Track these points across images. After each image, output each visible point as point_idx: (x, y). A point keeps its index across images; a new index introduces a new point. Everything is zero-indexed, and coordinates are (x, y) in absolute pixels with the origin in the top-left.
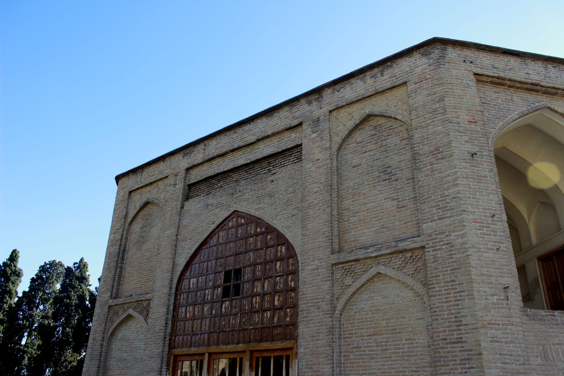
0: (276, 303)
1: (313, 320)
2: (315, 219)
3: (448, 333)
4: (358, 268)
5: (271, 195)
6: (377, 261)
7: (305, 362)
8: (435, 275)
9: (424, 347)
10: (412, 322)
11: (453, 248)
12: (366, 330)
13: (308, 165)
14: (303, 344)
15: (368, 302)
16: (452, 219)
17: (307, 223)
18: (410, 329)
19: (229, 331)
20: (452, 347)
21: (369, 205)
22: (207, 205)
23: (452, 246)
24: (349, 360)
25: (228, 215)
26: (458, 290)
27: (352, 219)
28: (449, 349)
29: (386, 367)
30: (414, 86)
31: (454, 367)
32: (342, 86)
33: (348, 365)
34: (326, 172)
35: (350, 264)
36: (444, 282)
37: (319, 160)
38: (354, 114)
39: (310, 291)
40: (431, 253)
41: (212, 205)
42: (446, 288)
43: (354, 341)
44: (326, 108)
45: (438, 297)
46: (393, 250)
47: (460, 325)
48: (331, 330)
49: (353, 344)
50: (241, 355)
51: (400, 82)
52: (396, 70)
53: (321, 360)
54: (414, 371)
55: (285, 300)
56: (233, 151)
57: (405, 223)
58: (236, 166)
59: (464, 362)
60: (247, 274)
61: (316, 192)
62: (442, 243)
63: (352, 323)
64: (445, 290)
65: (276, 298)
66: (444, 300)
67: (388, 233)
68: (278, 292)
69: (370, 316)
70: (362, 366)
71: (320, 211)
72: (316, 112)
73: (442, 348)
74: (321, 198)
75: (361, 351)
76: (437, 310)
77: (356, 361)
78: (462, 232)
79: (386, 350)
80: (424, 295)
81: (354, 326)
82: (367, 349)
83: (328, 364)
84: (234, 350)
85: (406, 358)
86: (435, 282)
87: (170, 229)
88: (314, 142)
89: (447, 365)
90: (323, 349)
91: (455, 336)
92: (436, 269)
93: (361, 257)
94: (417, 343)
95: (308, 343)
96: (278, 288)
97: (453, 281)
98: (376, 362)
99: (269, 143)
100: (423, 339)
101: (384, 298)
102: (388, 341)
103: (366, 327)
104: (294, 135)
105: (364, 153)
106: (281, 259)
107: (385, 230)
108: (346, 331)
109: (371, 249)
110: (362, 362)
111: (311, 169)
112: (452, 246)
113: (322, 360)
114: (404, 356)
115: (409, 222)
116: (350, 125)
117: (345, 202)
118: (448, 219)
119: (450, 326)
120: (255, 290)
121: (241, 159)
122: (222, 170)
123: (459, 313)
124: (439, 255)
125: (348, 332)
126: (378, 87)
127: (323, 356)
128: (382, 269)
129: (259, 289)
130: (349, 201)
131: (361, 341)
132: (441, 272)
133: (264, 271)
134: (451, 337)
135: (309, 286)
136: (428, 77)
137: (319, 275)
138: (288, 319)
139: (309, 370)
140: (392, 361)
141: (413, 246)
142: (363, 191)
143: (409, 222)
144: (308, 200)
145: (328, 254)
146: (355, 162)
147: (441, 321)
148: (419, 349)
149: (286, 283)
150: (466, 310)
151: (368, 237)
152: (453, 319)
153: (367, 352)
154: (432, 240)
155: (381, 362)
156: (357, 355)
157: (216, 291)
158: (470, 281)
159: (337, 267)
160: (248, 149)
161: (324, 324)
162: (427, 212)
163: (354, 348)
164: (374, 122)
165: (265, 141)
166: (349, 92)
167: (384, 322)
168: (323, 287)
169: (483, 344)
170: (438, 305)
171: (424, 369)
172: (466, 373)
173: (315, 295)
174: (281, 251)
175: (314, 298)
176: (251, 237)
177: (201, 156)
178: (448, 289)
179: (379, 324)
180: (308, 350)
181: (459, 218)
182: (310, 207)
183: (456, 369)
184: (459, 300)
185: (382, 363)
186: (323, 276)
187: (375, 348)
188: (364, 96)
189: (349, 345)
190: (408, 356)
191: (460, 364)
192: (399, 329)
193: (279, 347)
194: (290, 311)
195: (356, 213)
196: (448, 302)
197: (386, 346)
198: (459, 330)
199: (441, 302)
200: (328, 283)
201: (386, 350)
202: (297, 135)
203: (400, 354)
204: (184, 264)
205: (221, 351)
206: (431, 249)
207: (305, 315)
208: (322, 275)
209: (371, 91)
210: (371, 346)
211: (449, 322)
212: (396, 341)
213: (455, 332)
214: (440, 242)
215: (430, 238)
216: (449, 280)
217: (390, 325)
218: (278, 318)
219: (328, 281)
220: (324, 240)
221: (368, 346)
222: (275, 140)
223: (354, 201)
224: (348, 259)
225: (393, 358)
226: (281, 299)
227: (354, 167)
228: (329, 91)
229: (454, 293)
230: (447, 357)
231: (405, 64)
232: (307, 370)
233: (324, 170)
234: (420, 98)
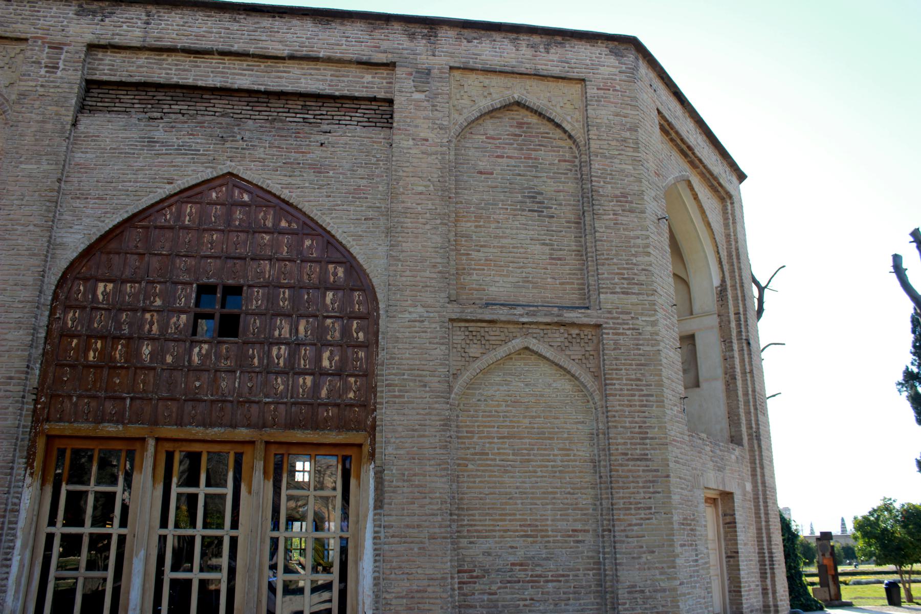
0: (326, 363)
1: (413, 403)
2: (417, 237)
3: (629, 446)
4: (492, 333)
5: (318, 169)
6: (524, 330)
7: (397, 470)
8: (615, 367)
9: (585, 461)
10: (568, 426)
11: (641, 337)
12: (496, 429)
13: (405, 143)
14: (393, 440)
15: (501, 388)
16: (641, 297)
17: (400, 239)
18: (566, 435)
19: (212, 402)
20: (634, 465)
21: (504, 241)
22: (152, 142)
23: (640, 334)
24: (467, 471)
25: (210, 176)
26: (645, 392)
27: (474, 254)
28: (630, 467)
29: (527, 485)
30: (595, 91)
31: (636, 490)
32: (475, 35)
33: (465, 479)
34: (439, 166)
35: (479, 324)
36: (627, 380)
37: (427, 140)
38: (492, 90)
39: (407, 355)
40: (610, 336)
41: (164, 144)
42: (629, 387)
43: (476, 444)
44: (442, 61)
45: (618, 397)
46: (556, 319)
47: (646, 438)
48: (446, 424)
49: (475, 448)
50: (239, 449)
51: (575, 75)
52: (570, 55)
53: (428, 468)
54: (569, 493)
55: (343, 360)
56: (223, 53)
57: (561, 284)
58: (228, 85)
59: (648, 484)
60: (256, 300)
61: (421, 193)
62: (626, 327)
63: (473, 416)
64: (628, 390)
65: (326, 355)
66: (626, 403)
67: (535, 291)
68: (331, 345)
69: (503, 408)
70: (489, 482)
71: (428, 227)
72: (423, 57)
73: (621, 465)
74: (430, 206)
75: (487, 460)
76: (617, 414)
77: (479, 473)
78: (653, 319)
79: (529, 461)
80: (594, 391)
81: (476, 421)
82: (498, 458)
83: (442, 476)
84: (226, 437)
85: (557, 474)
86: (614, 376)
87: (38, 163)
88: (418, 107)
89: (628, 488)
90: (432, 452)
91: (638, 451)
92: (617, 359)
93: (503, 318)
94: (574, 455)
95: (403, 440)
96: (329, 338)
97: (639, 380)
98: (512, 477)
99: (313, 72)
100: (583, 451)
101: (527, 385)
102: (533, 449)
103: (496, 425)
104: (368, 78)
105: (498, 157)
106: (335, 288)
107: (531, 285)
108: (462, 427)
109: (519, 311)
110: (490, 476)
111: (411, 151)
112: (640, 334)
113: (431, 469)
114: (555, 472)
115: (568, 283)
116: (485, 104)
117: (463, 224)
118: (634, 296)
119: (633, 438)
120: (277, 333)
121: (243, 77)
122: (190, 81)
123: (645, 422)
124: (621, 342)
125: (465, 429)
126: (539, 67)
127: (432, 462)
128: (533, 344)
129: (286, 333)
130: (469, 224)
131: (487, 445)
132: (624, 364)
133: (293, 300)
134: (634, 452)
135: (407, 346)
136: (618, 88)
137: (426, 332)
138: (351, 395)
139: (406, 484)
140: (538, 477)
141: (585, 320)
142: (495, 217)
143: (568, 283)
144: (403, 202)
145: (442, 301)
146: (483, 165)
147: (620, 429)
148: (578, 463)
149: (346, 331)
150: (653, 420)
151: (501, 289)
152: (637, 430)
153: (498, 462)
154: (612, 318)
155: (521, 477)
156: (479, 465)
157: (175, 319)
158: (660, 385)
159: (455, 324)
160: (263, 65)
161: (434, 412)
162: (607, 279)
163: (476, 454)
164: (522, 115)
165: (305, 65)
166: (488, 51)
167: (527, 421)
168: (433, 352)
169: (672, 465)
170: (618, 408)
171: (583, 491)
172: (650, 498)
173: (417, 362)
174: (335, 274)
175: (416, 367)
176: (265, 233)
177: (138, 33)
178: (632, 390)
179: (518, 422)
180: (402, 452)
181: (651, 298)
182: (409, 215)
183: (638, 493)
184: (645, 406)
185: (520, 480)
186: (432, 335)
187: (511, 457)
188: (516, 70)
189: (468, 448)
190: (560, 472)
191: (644, 487)
192: (550, 433)
193: (333, 441)
194: (356, 382)
195: (481, 246)
196: (631, 406)
197: (529, 455)
198: (644, 444)
199: (623, 405)
200: (443, 347)
201: (529, 461)
202: (376, 80)
203: (550, 469)
204: (82, 247)
205: (191, 438)
206: (611, 331)
207: (397, 393)
208: (431, 332)
209: (526, 67)
210: (504, 454)
211: (631, 432)
212: (545, 449)
213: (638, 446)
214: (625, 324)
215: (609, 315)
216: (633, 377)
217: (536, 426)
218: (330, 391)
219: (443, 344)
220: (435, 276)
221: (499, 454)
222: (327, 72)
223: (480, 226)
224: (479, 317)
225: (539, 474)
226: (337, 358)
227: (481, 173)
228: (452, 33)
229: (640, 396)
230: (627, 477)
231: (583, 53)
232: (400, 484)
233: (437, 161)
234: (603, 112)
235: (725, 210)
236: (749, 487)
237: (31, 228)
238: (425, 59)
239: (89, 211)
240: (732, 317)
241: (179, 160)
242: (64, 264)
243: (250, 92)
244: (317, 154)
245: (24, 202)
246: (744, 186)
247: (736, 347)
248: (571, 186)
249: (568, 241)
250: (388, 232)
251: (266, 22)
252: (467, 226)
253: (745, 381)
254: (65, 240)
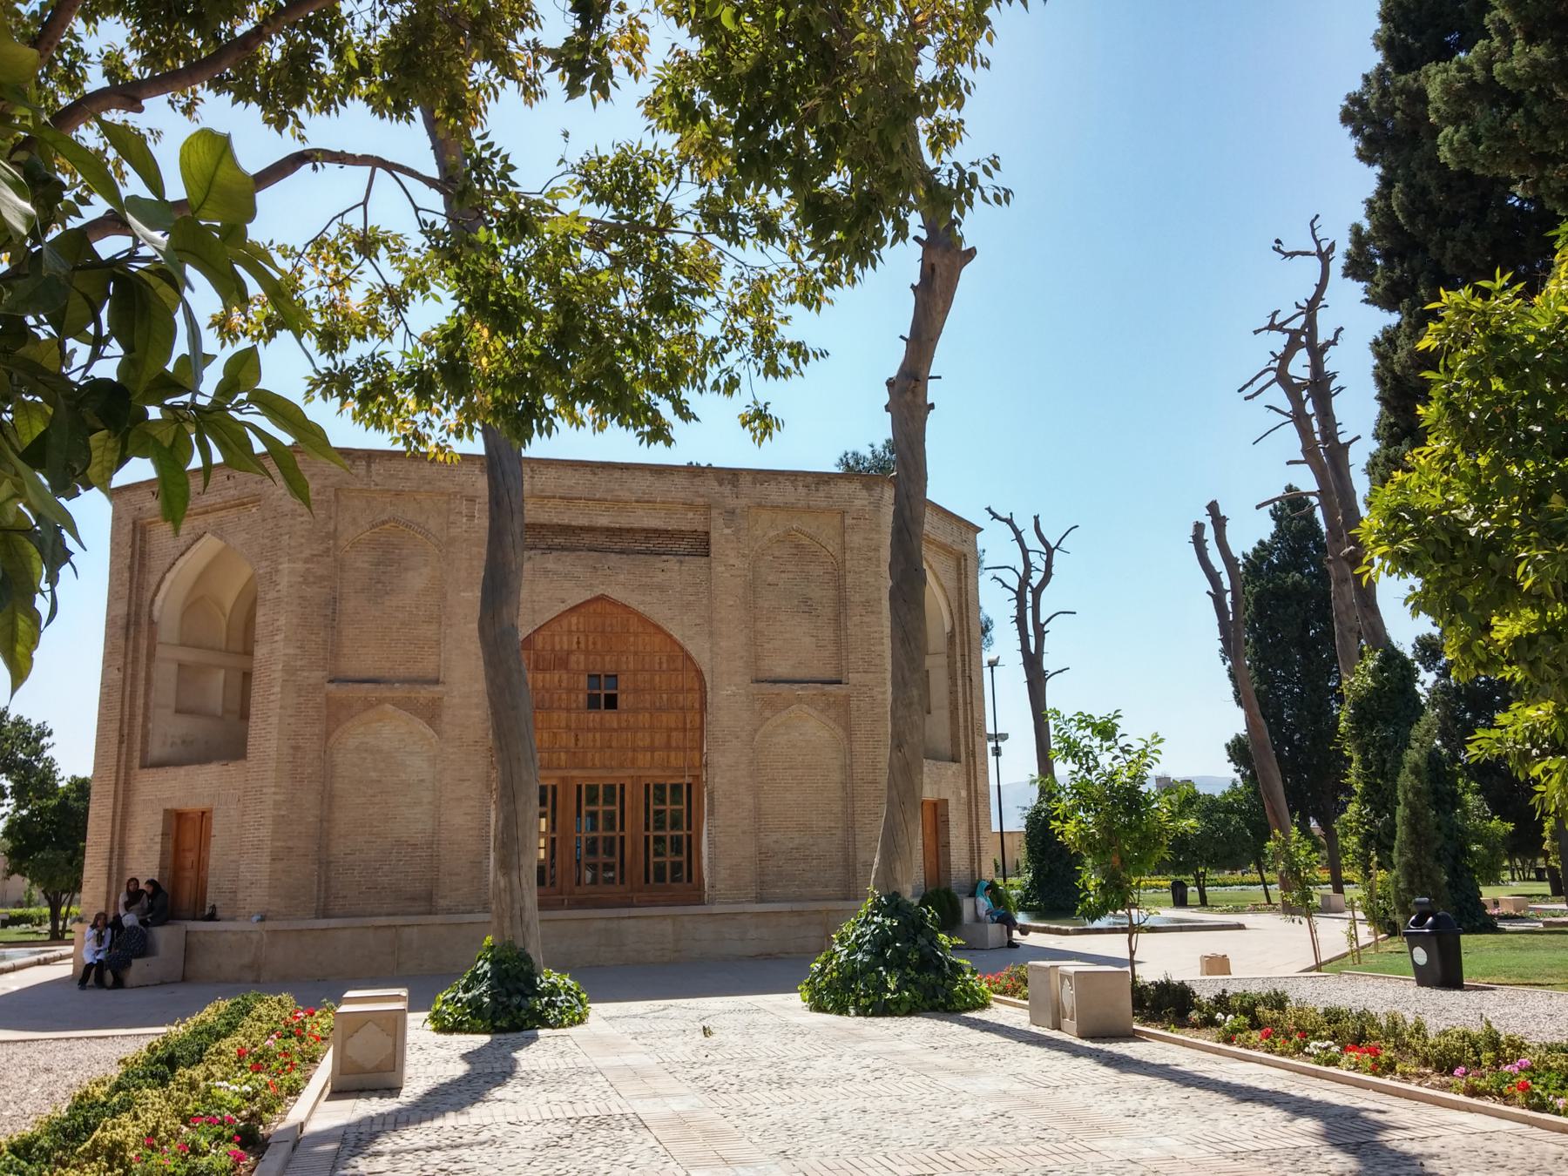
5: (662, 589)
22: (546, 571)
100: (836, 777)
146: (770, 579)
166: (774, 493)
235: (959, 565)
236: (964, 793)
238: (731, 502)
240: (958, 658)
241: (567, 585)
243: (608, 529)
244: (659, 578)
246: (979, 535)
247: (960, 682)
248: (832, 593)
249: (828, 634)
250: (711, 634)
251: (617, 474)
252: (761, 625)
253: (965, 711)
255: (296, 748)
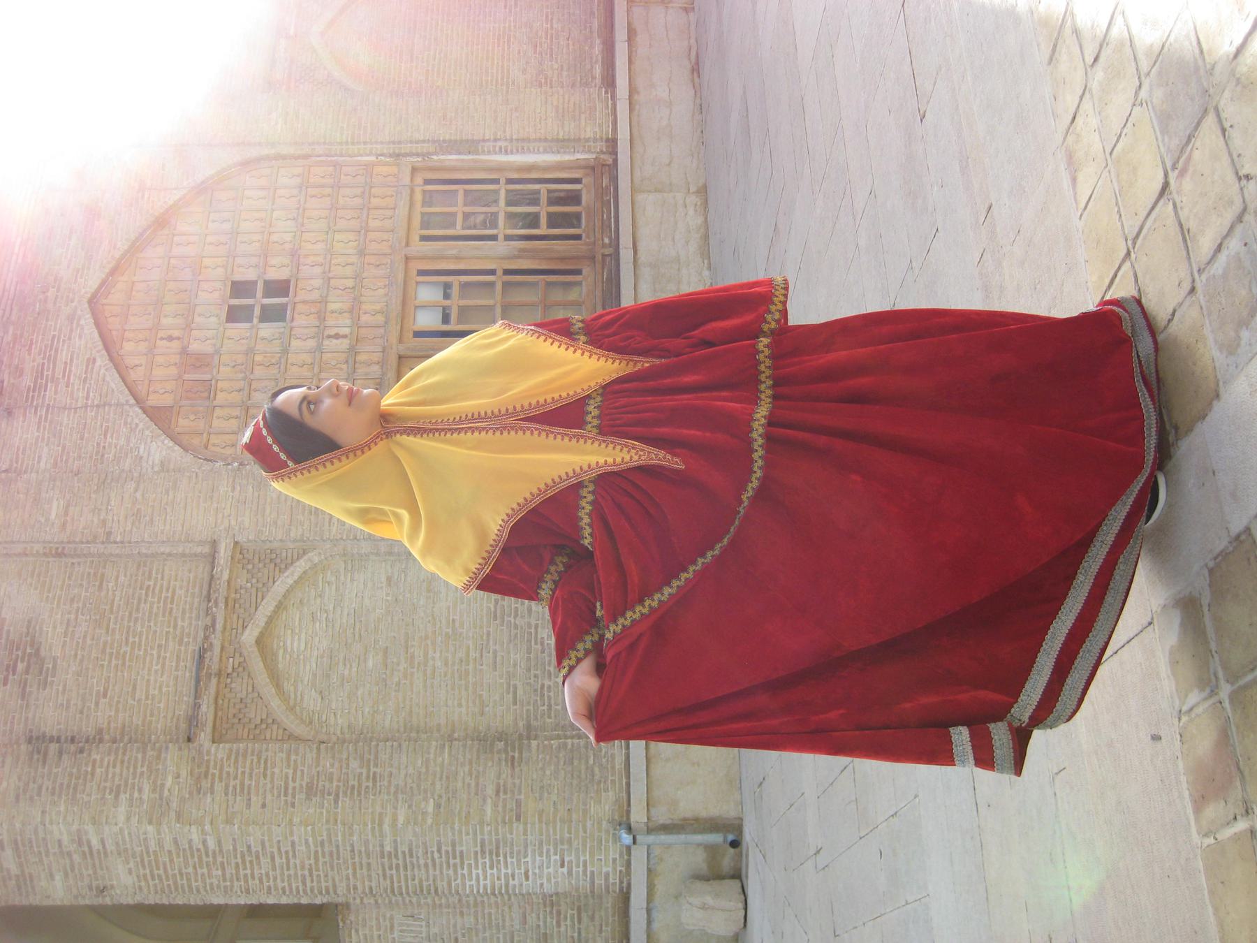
237: (138, 495)
239: (122, 442)
242: (189, 458)
245: (104, 508)
254: (157, 462)
255: (311, 790)
